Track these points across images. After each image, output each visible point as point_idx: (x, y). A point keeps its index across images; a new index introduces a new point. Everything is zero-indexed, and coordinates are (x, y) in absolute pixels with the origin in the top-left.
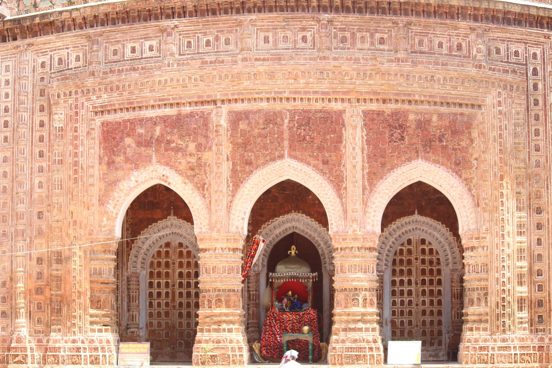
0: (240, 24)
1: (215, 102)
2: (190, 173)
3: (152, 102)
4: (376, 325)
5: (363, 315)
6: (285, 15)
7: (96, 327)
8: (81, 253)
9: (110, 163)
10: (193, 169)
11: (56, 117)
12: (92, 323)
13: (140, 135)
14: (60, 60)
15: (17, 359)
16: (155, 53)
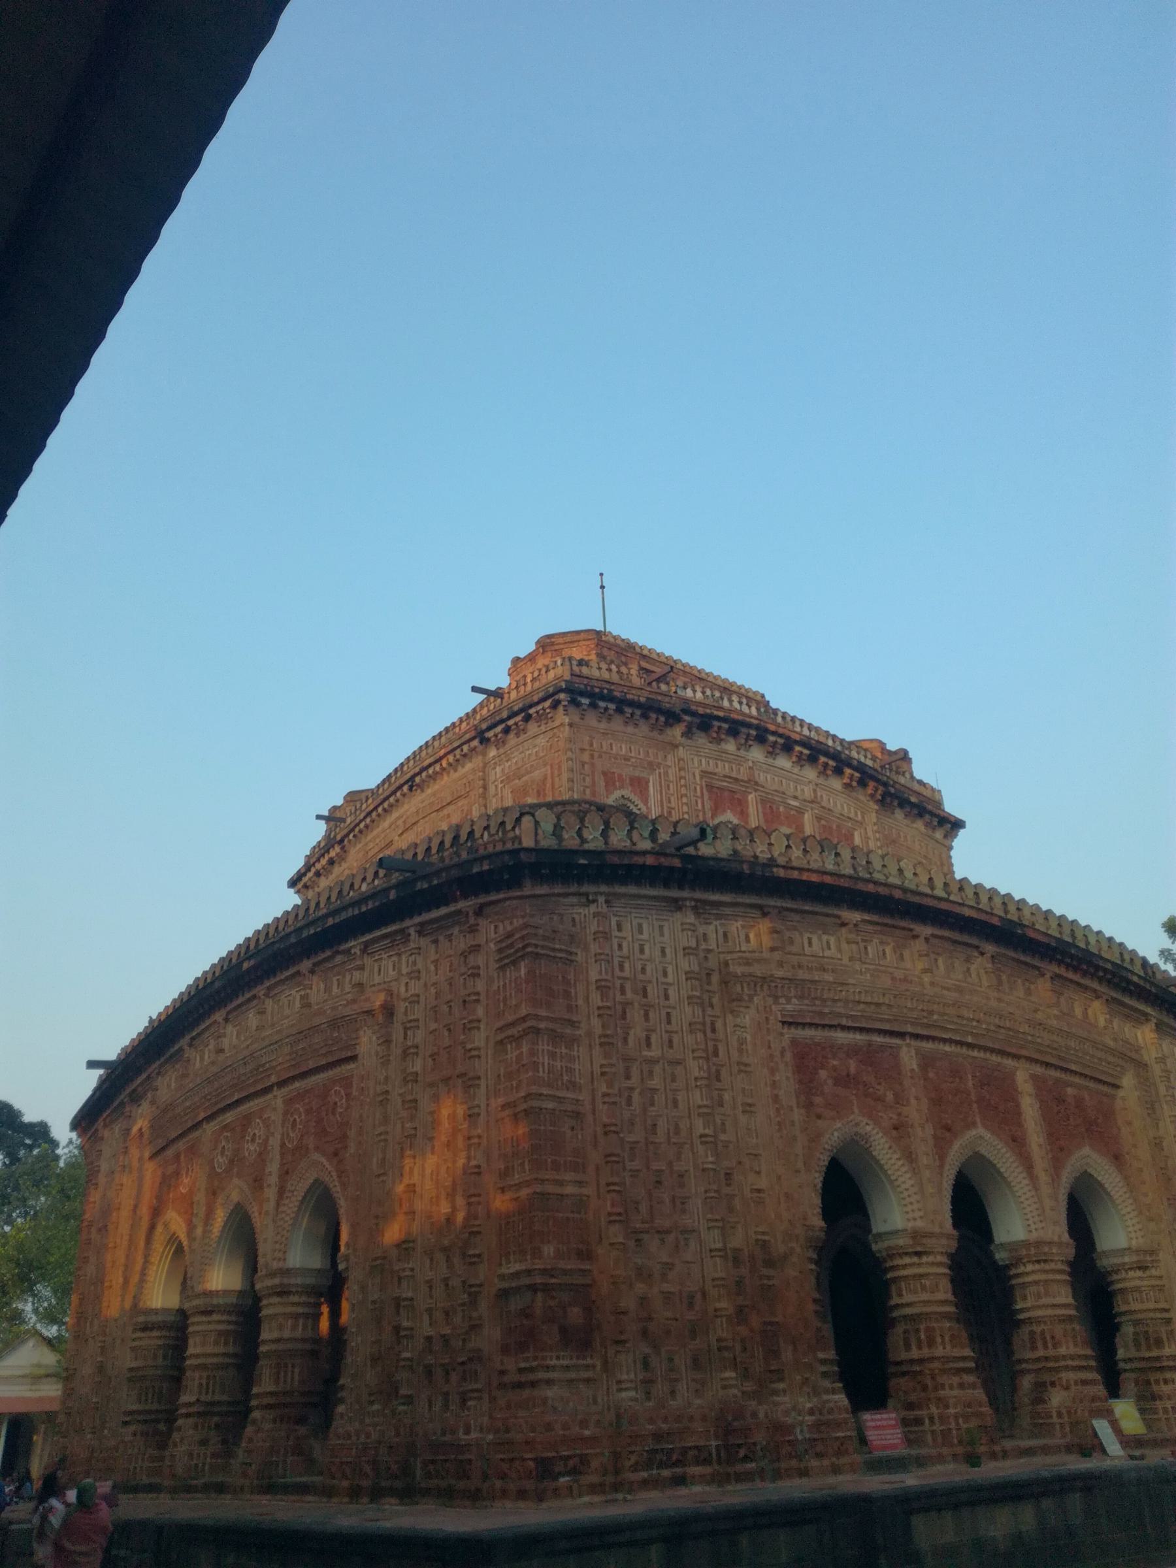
0: (915, 937)
1: (901, 1035)
2: (894, 1132)
3: (844, 1022)
4: (1096, 1376)
5: (1086, 1357)
6: (956, 936)
7: (827, 1384)
8: (798, 1250)
9: (809, 1106)
10: (896, 1128)
11: (739, 1020)
12: (825, 1375)
13: (835, 1069)
14: (725, 935)
15: (742, 1453)
16: (832, 953)
